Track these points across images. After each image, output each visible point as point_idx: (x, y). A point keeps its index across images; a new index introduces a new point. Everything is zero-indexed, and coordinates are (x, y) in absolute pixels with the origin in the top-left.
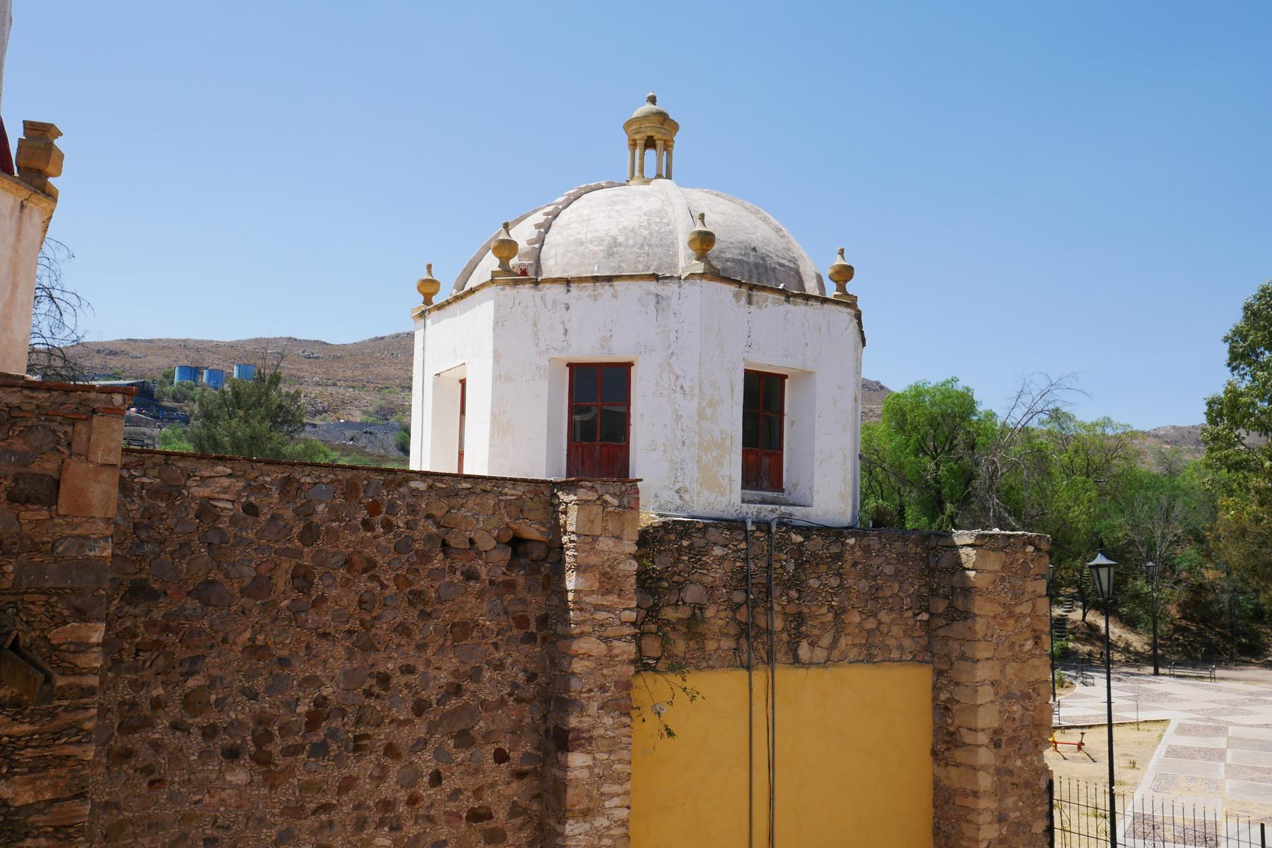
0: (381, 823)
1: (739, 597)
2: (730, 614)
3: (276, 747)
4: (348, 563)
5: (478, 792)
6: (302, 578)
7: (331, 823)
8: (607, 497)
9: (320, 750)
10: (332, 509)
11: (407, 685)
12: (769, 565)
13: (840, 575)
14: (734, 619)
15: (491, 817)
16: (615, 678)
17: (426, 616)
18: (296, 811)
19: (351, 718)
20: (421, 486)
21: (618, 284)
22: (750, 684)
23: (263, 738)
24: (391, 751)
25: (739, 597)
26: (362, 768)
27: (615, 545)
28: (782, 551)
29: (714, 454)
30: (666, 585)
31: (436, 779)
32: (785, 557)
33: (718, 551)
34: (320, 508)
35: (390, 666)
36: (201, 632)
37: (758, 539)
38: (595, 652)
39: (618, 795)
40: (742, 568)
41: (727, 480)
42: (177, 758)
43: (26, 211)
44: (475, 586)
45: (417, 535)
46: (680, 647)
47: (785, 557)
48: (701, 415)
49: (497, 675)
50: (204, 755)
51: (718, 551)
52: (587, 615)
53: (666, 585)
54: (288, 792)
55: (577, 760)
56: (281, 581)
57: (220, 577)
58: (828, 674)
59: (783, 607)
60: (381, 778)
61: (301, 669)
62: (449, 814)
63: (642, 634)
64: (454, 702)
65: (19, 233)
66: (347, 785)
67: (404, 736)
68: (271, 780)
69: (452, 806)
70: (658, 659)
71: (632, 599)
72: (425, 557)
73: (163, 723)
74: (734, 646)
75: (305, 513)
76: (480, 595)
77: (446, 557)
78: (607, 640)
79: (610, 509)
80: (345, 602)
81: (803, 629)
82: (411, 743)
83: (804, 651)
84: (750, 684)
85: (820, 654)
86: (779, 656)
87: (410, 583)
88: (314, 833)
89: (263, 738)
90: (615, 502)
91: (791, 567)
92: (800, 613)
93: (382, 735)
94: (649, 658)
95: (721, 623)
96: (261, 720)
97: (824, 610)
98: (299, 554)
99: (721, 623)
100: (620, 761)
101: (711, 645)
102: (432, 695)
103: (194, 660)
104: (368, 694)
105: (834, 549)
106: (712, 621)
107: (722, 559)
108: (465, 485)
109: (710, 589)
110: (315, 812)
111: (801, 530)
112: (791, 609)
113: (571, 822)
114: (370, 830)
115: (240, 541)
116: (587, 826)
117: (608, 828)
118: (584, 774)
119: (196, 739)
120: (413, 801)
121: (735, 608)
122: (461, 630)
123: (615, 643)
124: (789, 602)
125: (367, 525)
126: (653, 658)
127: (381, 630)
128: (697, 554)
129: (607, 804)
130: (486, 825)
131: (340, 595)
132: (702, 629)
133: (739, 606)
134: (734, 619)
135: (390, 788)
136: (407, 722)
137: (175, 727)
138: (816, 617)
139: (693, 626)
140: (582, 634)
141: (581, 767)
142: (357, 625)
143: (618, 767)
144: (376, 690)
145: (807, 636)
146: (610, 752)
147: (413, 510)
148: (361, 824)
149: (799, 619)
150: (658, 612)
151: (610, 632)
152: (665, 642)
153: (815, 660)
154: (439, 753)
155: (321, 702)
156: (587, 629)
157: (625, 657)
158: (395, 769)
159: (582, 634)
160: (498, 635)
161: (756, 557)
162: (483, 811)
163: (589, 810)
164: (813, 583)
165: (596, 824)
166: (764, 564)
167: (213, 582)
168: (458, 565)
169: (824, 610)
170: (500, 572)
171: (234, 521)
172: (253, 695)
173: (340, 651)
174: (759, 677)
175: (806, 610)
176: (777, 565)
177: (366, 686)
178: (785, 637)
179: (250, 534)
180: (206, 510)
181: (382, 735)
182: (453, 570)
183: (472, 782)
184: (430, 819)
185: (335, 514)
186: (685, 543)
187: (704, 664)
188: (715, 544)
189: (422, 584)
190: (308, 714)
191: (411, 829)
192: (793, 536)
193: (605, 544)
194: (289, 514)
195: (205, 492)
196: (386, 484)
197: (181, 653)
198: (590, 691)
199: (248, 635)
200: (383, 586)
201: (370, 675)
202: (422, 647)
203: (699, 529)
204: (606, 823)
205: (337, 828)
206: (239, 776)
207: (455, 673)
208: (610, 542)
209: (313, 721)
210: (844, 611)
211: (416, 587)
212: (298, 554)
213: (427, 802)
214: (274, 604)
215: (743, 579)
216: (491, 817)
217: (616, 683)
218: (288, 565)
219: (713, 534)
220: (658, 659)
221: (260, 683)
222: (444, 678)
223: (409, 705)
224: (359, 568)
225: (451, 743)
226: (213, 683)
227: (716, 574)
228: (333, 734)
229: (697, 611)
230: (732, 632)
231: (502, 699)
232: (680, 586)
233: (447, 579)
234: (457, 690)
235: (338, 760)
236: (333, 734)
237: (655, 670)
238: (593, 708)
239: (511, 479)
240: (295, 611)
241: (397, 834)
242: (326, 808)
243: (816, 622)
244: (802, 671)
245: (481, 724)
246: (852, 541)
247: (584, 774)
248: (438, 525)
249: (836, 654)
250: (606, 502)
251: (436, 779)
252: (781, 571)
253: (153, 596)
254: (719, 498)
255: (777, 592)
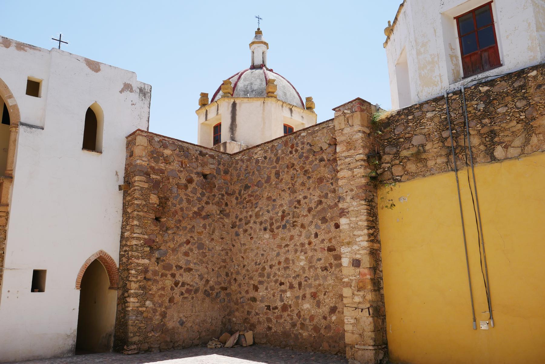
0: (302, 251)
1: (445, 134)
2: (441, 144)
3: (274, 227)
4: (288, 167)
5: (330, 240)
6: (277, 174)
7: (288, 250)
8: (346, 111)
9: (284, 227)
10: (283, 151)
11: (306, 203)
12: (463, 112)
13: (524, 98)
14: (444, 146)
15: (335, 250)
16: (357, 185)
17: (309, 178)
18: (280, 246)
19: (291, 216)
20: (303, 134)
21: (399, 18)
22: (457, 177)
23: (272, 224)
24: (303, 226)
25: (445, 134)
26: (295, 232)
27: (351, 129)
28: (473, 100)
29: (428, 68)
30: (402, 140)
31: (316, 235)
32: (476, 102)
33: (429, 115)
34: (280, 151)
35: (301, 197)
36: (257, 195)
37: (454, 100)
38: (346, 176)
39: (362, 236)
40: (446, 118)
41: (438, 78)
42: (255, 231)
43: (265, 104)
44: (323, 163)
45: (304, 151)
46: (412, 167)
47: (476, 102)
48: (419, 53)
49: (333, 195)
50: (260, 230)
51: (429, 115)
52: (342, 161)
53: (402, 140)
54: (278, 240)
55: (343, 221)
56: (273, 176)
57: (260, 179)
58: (520, 165)
59: (479, 131)
60: (300, 236)
61: (279, 202)
62: (321, 248)
63: (392, 166)
64: (320, 207)
65: (264, 110)
66: (292, 238)
67: (306, 221)
68: (274, 236)
69: (322, 245)
70: (401, 176)
71: (360, 149)
72: (307, 158)
73: (252, 222)
74: (447, 161)
75: (276, 155)
76: (325, 166)
77: (314, 155)
78: (351, 170)
79: (347, 116)
80: (287, 179)
81: (496, 139)
82: (308, 223)
83: (499, 152)
84: (457, 177)
85: (512, 152)
86: (478, 159)
87: (304, 168)
88: (285, 253)
89: (272, 224)
90: (349, 112)
91: (481, 106)
92: (492, 132)
93: (300, 221)
94: (397, 176)
95: (435, 150)
96: (271, 219)
97: (514, 123)
98: (275, 167)
99: (435, 150)
100: (361, 220)
101: (431, 163)
102: (313, 205)
103: (256, 203)
104: (295, 207)
105: (516, 85)
106: (430, 151)
107: (432, 119)
108: (317, 128)
109: (428, 136)
110: (285, 247)
111: (486, 84)
112: (485, 130)
113: (343, 247)
114: (298, 253)
115: (264, 167)
116: (350, 249)
117: (359, 250)
118: (346, 227)
119: (258, 225)
120: (310, 243)
121: (443, 140)
122: (320, 180)
123: (355, 170)
124: (482, 127)
125: (291, 152)
126: (398, 176)
127: (297, 186)
128: (418, 122)
129: (358, 240)
130: (334, 253)
131: (286, 177)
132: (424, 156)
133: (446, 139)
134: (444, 146)
135: (303, 239)
136: (307, 216)
137: (255, 222)
138: (505, 130)
139: (419, 156)
140: (341, 169)
141: (345, 224)
142: (290, 185)
143: (360, 223)
144: (297, 206)
145: (500, 143)
146: (357, 217)
147: (303, 143)
148: (296, 251)
149: (493, 134)
150: (399, 154)
151: (352, 166)
152: (404, 167)
153: (510, 157)
154: (317, 226)
155: (284, 212)
156: (342, 167)
157: (359, 175)
158: (304, 232)
159: (341, 169)
160: (332, 179)
161: (455, 110)
162: (332, 247)
163: (350, 242)
164: (501, 110)
165: (353, 248)
166: (461, 111)
167: (259, 181)
168: (318, 157)
169: (514, 123)
170: (330, 156)
171: (263, 162)
172: (268, 211)
173: (287, 195)
174: (463, 174)
175: (496, 128)
176: (470, 109)
177: (294, 205)
178: (482, 147)
179: (265, 165)
180: (257, 161)
181: (300, 221)
182: (316, 159)
183: (328, 236)
184: (316, 250)
185: (283, 152)
186: (410, 117)
187: (428, 173)
188: (427, 112)
189: (307, 167)
190: (282, 215)
191: (310, 254)
192: (481, 88)
193: (347, 130)
194: (273, 156)
195: (256, 157)
196: (295, 137)
197: (254, 202)
198: (347, 192)
199: (267, 194)
200: (297, 171)
201: (296, 201)
202: (309, 189)
203: (417, 108)
204: (358, 248)
205: (290, 251)
206: (267, 236)
207: (320, 196)
208: (349, 129)
209: (283, 217)
210: (534, 119)
211: (305, 169)
212: (275, 167)
213: (314, 244)
214: (271, 184)
215: (447, 123)
216: (335, 250)
217: (356, 187)
218: (274, 171)
219: (426, 107)
220: (401, 176)
221: (270, 208)
222: (316, 199)
223: (306, 210)
224: (290, 167)
225: (320, 222)
226: (261, 208)
227: (430, 127)
228: (287, 222)
229: (421, 148)
230: (443, 153)
231: (336, 203)
232: (409, 139)
233: (314, 163)
234: (320, 202)
235: (289, 230)
236: (287, 222)
237: (400, 181)
238: (348, 199)
239: (330, 120)
240: (276, 184)
241: (306, 255)
242: (287, 245)
243: (506, 133)
244: (496, 165)
245: (329, 214)
246: (534, 73)
247: (346, 227)
248: (311, 146)
249: (528, 149)
250: (345, 113)
251: (316, 235)
252: (474, 111)
253: (249, 187)
254: (435, 88)
255: (472, 124)
